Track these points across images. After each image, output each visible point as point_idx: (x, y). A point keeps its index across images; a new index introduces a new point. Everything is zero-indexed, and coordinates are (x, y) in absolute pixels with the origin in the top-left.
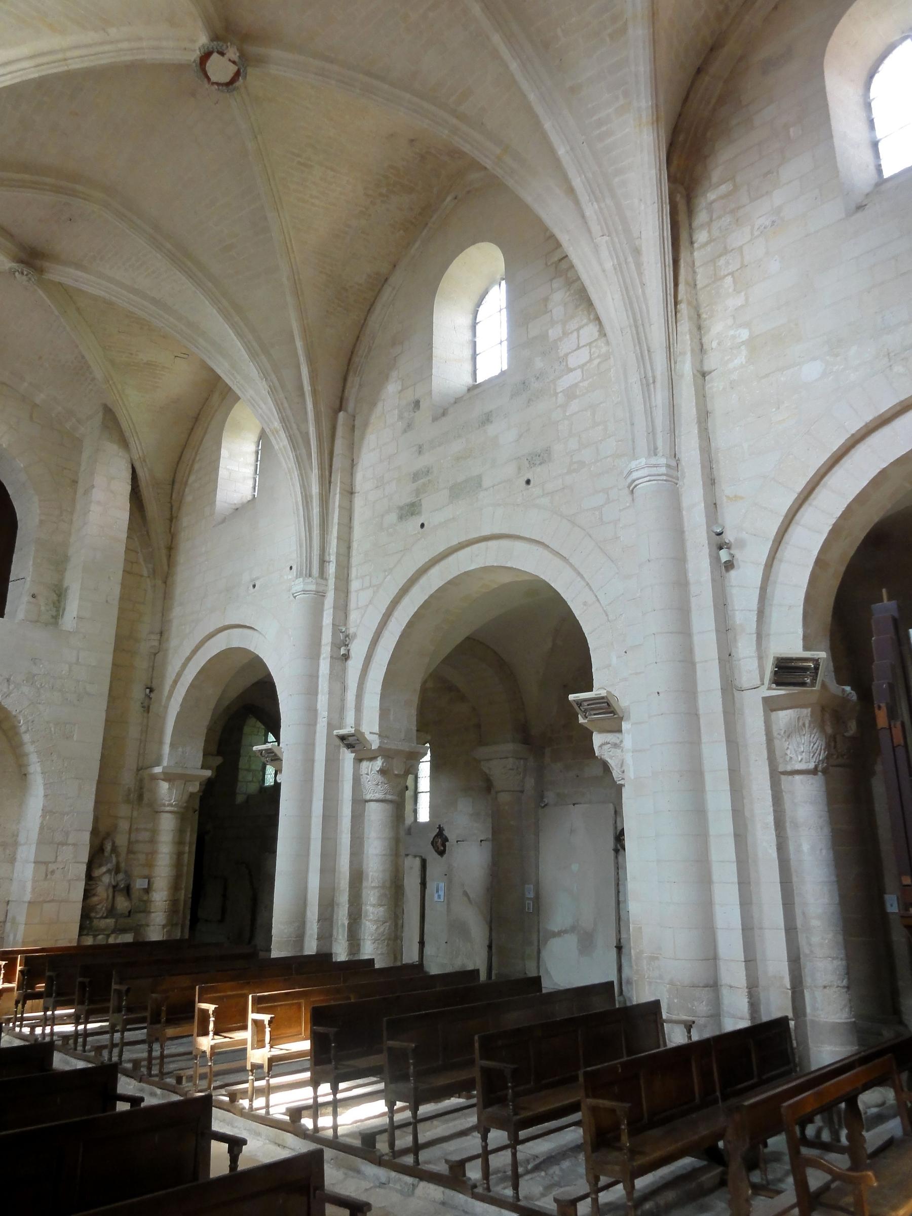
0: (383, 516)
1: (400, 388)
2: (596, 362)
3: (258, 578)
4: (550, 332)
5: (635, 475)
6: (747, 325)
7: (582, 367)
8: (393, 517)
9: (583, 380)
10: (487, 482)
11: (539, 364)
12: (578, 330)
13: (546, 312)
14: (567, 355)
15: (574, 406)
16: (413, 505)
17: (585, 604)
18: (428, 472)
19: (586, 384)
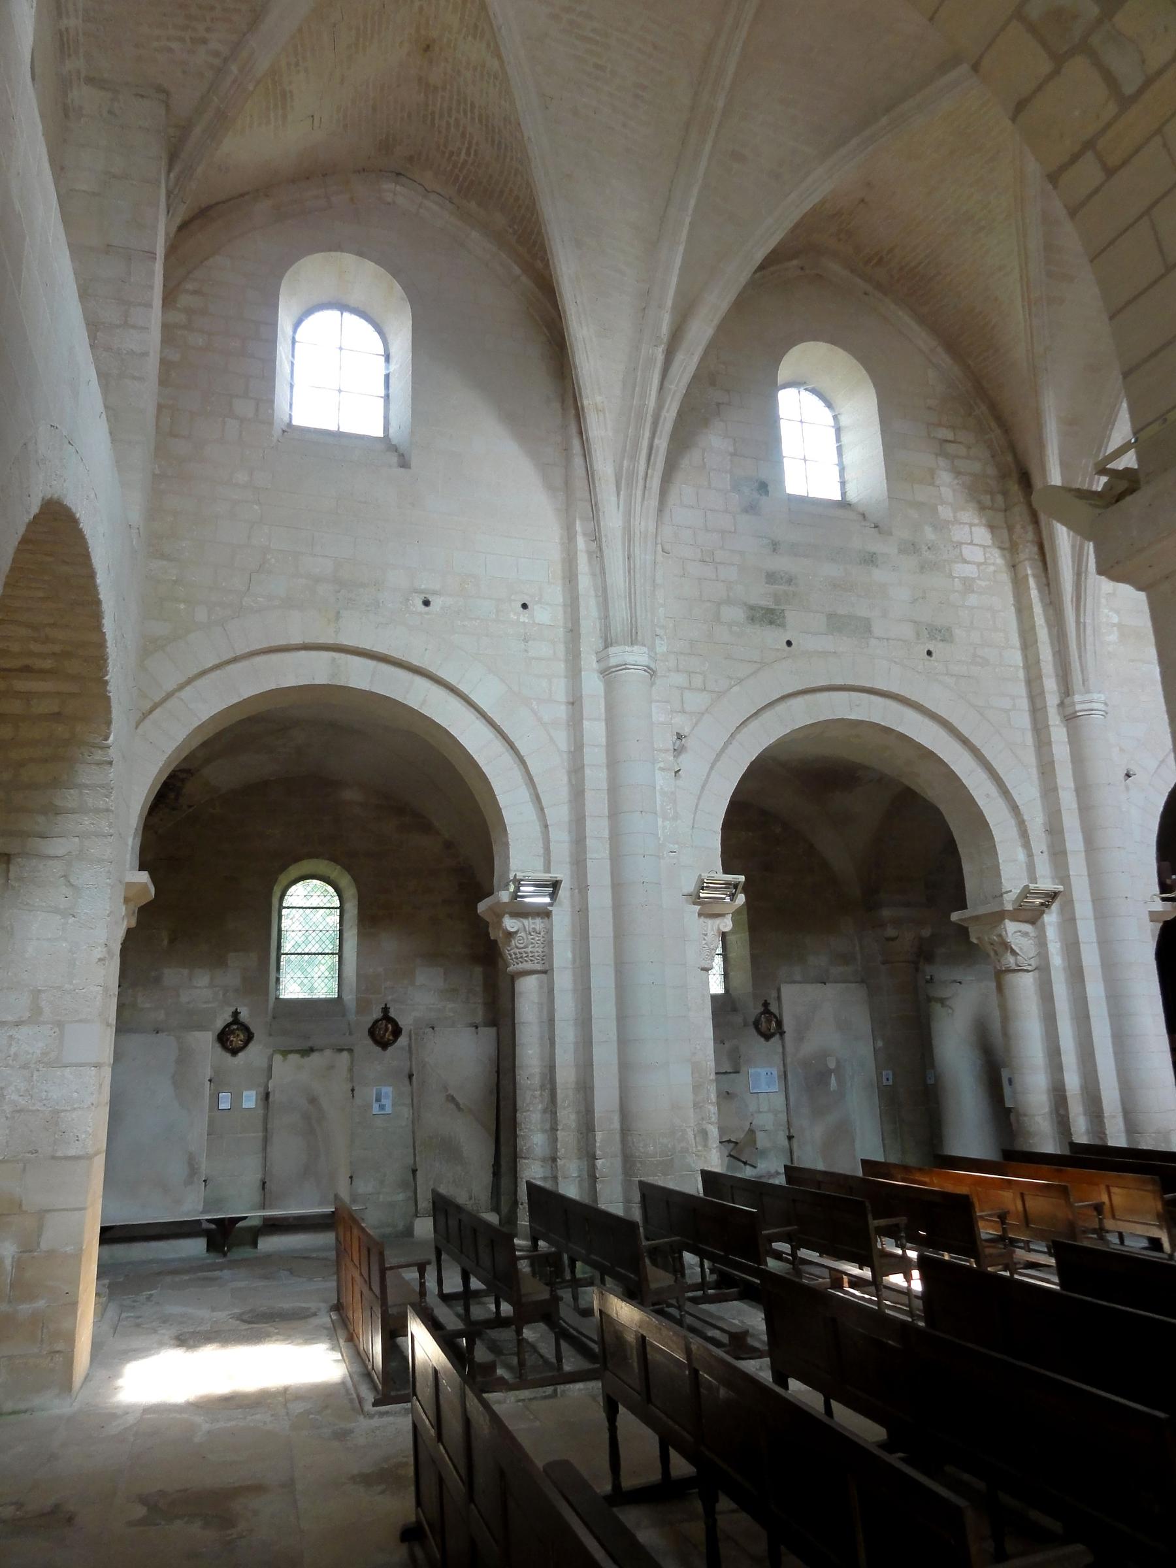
0: (719, 604)
1: (731, 449)
2: (992, 568)
3: (434, 593)
4: (940, 508)
5: (1095, 706)
6: (1117, 612)
7: (979, 564)
8: (736, 614)
9: (979, 578)
10: (877, 630)
11: (929, 534)
12: (971, 525)
13: (933, 484)
14: (960, 544)
15: (973, 600)
16: (771, 611)
17: (988, 796)
18: (790, 581)
19: (983, 584)
